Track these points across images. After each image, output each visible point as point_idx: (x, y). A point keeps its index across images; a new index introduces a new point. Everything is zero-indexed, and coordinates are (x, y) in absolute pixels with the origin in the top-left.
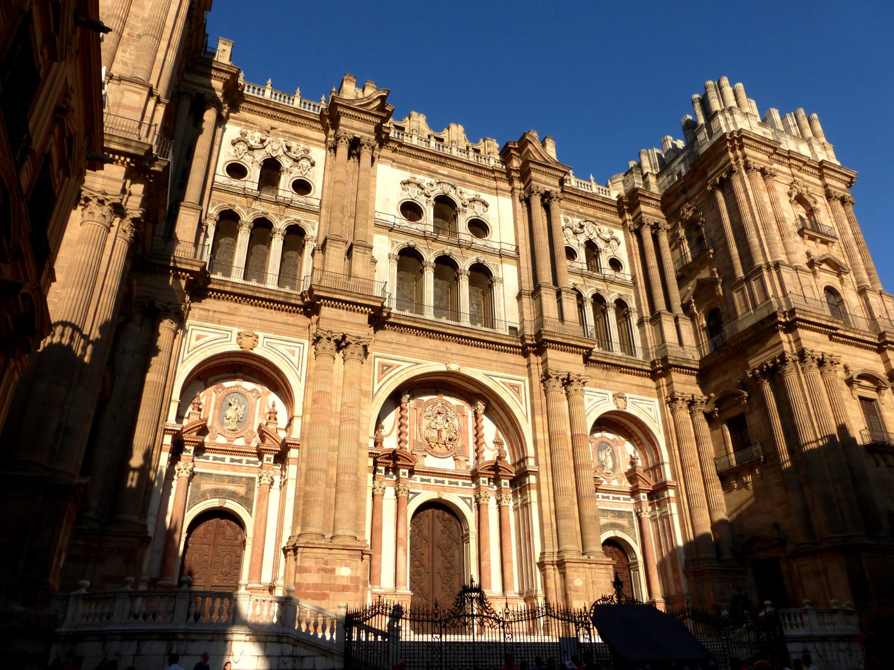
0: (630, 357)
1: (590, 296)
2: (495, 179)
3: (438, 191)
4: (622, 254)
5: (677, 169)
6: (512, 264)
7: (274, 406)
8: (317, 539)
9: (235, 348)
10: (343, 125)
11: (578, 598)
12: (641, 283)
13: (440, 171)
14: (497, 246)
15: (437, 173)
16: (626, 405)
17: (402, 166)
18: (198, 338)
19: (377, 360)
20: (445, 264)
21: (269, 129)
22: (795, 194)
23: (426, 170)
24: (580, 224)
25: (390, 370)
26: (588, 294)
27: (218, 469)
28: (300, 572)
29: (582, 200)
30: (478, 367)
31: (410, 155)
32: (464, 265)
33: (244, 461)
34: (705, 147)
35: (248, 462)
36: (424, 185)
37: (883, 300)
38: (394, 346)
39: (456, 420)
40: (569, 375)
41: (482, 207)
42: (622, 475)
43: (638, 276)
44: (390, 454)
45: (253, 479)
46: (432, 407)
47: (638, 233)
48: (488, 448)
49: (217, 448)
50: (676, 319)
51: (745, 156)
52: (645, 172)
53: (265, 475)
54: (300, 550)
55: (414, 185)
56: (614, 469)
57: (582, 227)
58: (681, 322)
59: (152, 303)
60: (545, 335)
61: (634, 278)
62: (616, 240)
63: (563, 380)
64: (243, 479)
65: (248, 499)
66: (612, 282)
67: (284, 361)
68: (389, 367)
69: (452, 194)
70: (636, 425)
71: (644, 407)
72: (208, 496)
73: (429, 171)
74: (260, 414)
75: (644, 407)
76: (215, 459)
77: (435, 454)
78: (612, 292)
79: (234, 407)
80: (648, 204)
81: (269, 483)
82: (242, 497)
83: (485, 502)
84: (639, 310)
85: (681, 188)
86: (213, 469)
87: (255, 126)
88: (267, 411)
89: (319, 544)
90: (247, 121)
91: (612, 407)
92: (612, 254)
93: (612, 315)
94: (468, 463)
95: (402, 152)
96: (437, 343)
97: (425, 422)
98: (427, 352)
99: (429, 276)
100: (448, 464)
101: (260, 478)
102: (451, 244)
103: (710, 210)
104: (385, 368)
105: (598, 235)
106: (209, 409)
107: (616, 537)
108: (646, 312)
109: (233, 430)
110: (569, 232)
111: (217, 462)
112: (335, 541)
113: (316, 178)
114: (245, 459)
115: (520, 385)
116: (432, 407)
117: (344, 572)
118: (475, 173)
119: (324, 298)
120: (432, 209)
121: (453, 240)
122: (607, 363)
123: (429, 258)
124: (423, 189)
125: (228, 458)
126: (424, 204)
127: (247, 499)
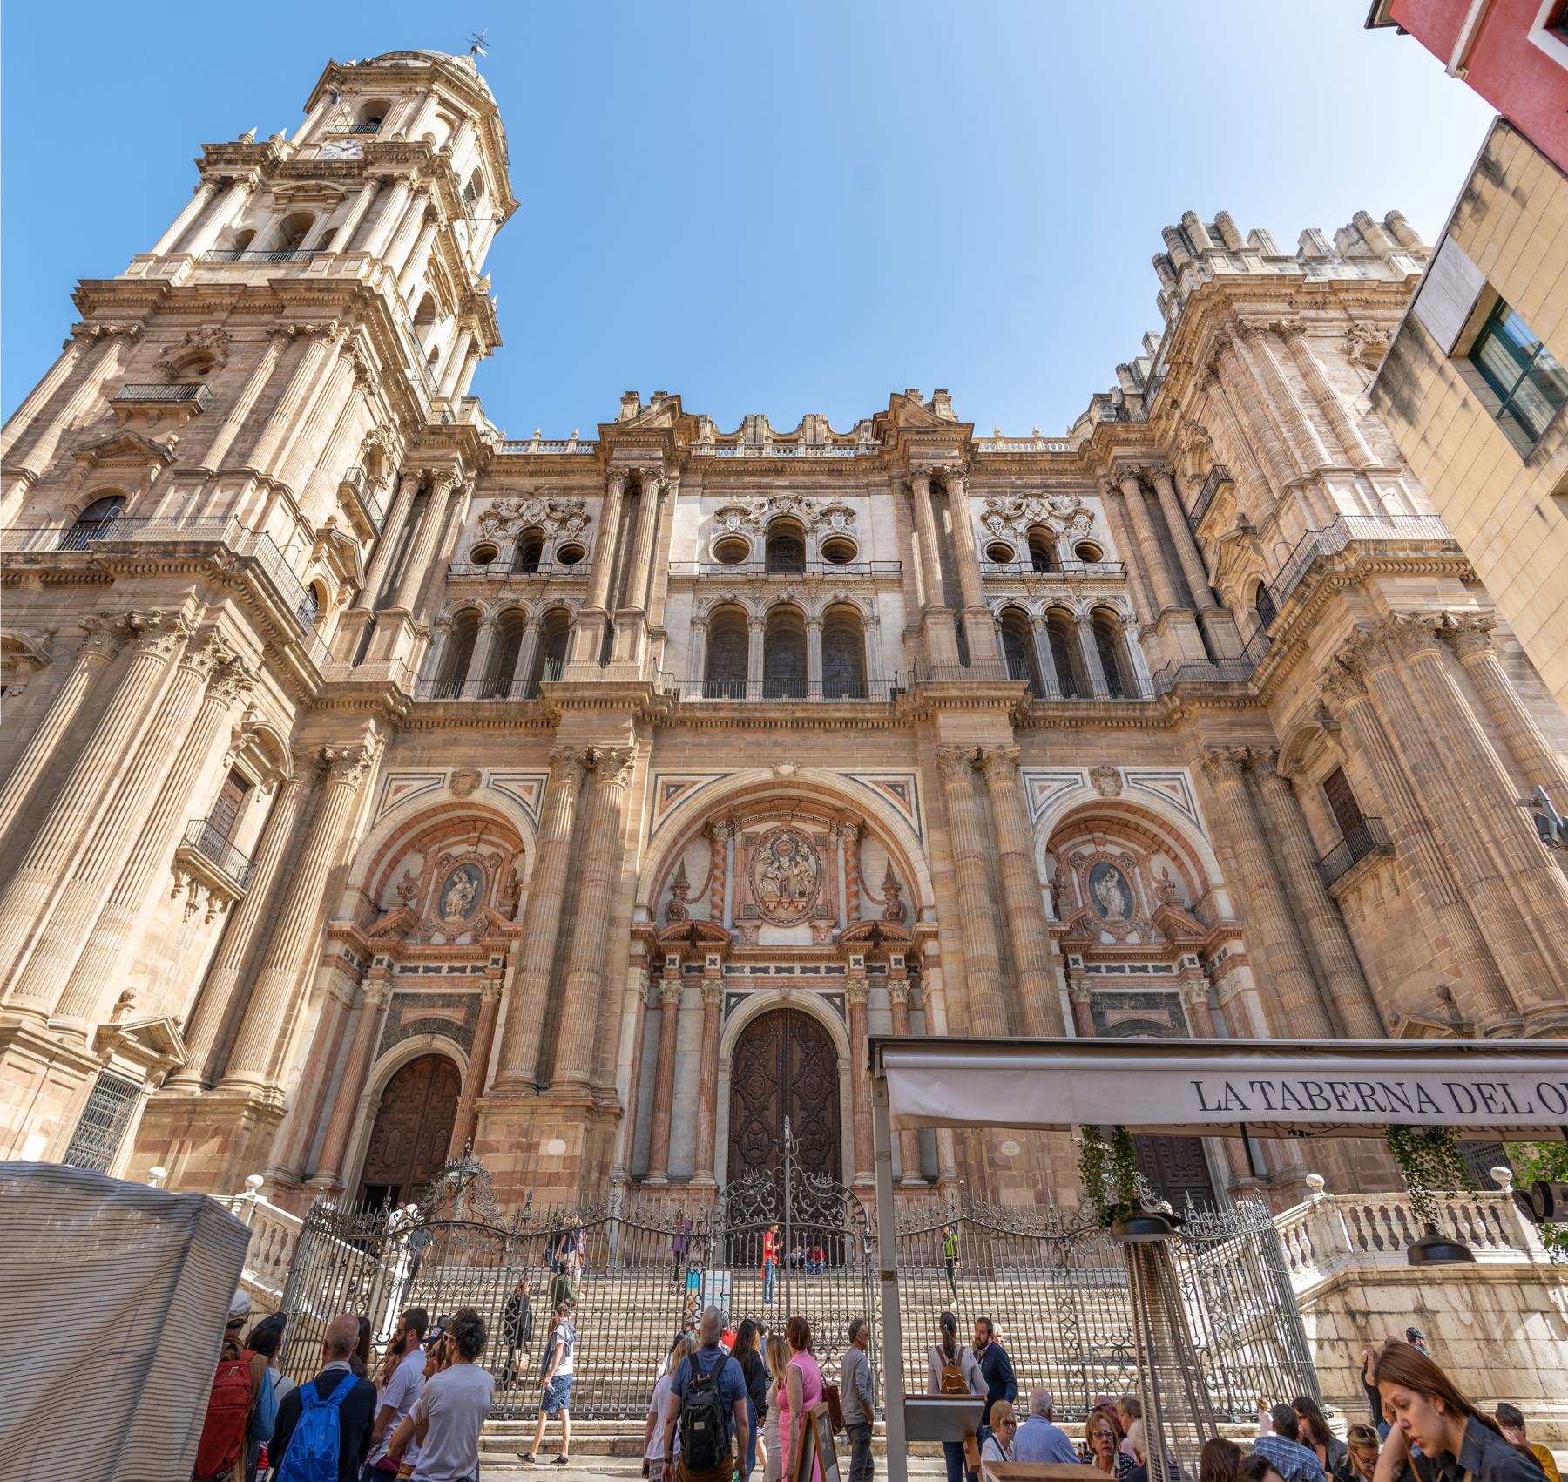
3: (775, 510)
7: (515, 872)
11: (1012, 1183)
14: (866, 569)
17: (718, 490)
31: (729, 472)
32: (814, 610)
36: (751, 508)
39: (812, 859)
41: (843, 518)
48: (873, 900)
69: (796, 511)
83: (860, 999)
94: (836, 932)
95: (717, 472)
96: (760, 736)
97: (760, 868)
98: (742, 754)
100: (799, 936)
102: (791, 584)
113: (587, 540)
117: (554, 1147)
118: (832, 472)
120: (763, 540)
121: (796, 577)
123: (756, 610)
126: (751, 536)
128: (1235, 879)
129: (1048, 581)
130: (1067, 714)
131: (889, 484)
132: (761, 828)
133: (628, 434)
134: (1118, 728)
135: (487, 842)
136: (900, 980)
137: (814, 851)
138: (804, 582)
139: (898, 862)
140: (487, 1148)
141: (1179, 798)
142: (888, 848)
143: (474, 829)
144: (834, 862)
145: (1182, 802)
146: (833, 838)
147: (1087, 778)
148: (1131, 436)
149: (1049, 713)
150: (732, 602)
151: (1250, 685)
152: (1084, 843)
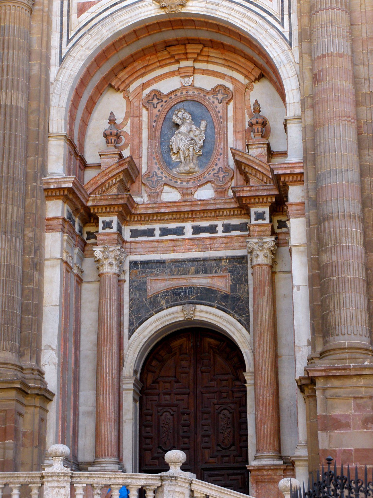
7: (257, 109)
8: (353, 359)
18: (82, 9)
27: (174, 251)
28: (325, 429)
33: (220, 229)
35: (227, 228)
45: (242, 259)
49: (162, 210)
53: (256, 247)
54: (320, 384)
64: (223, 263)
65: (239, 299)
67: (249, 14)
72: (163, 302)
76: (165, 232)
79: (183, 129)
81: (268, 261)
82: (225, 297)
86: (165, 251)
89: (355, 368)
101: (251, 253)
106: (141, 142)
109: (189, 173)
111: (170, 237)
114: (220, 224)
125: (188, 226)
127: (236, 299)
135: (205, 72)
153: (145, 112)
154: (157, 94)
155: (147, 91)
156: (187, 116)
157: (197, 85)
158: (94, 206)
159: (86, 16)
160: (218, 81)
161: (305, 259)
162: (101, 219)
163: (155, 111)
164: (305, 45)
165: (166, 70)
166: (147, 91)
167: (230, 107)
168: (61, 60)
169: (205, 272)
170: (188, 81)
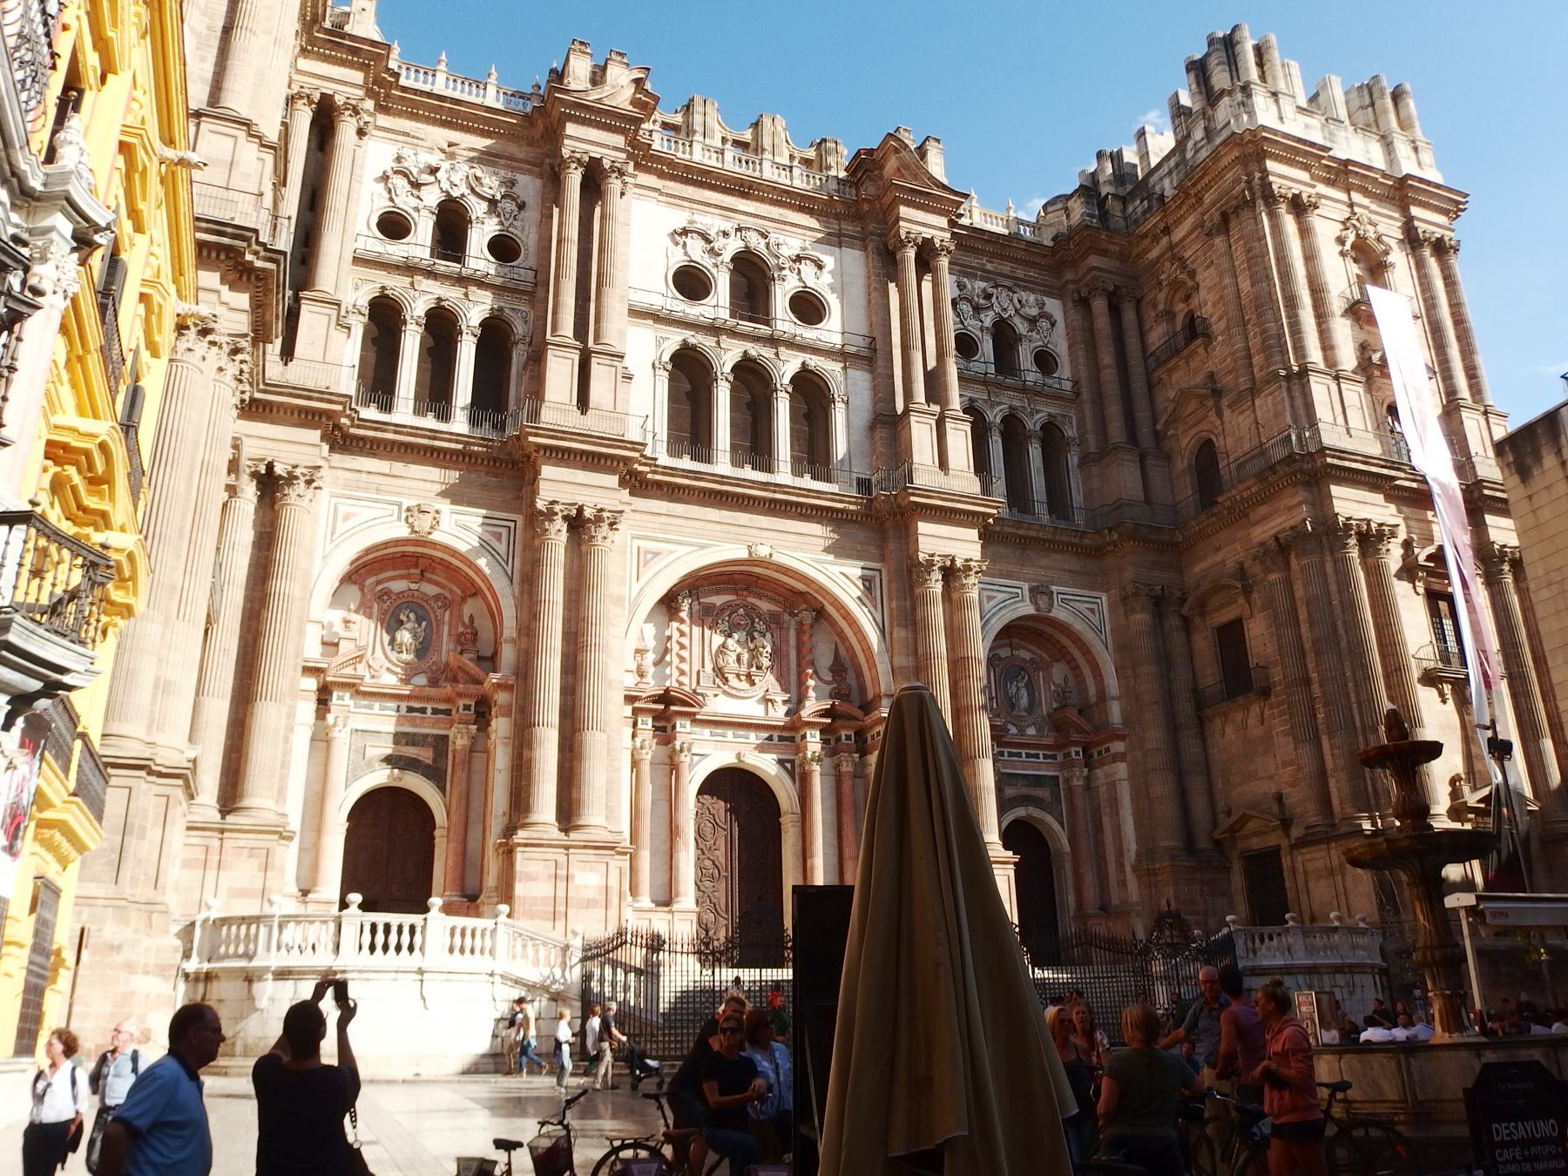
0: (1062, 525)
1: (998, 420)
2: (838, 217)
4: (1060, 345)
5: (1157, 188)
6: (863, 369)
9: (403, 532)
10: (571, 137)
12: (1086, 396)
13: (741, 208)
15: (735, 211)
16: (1052, 605)
18: (346, 518)
19: (637, 543)
20: (750, 376)
21: (445, 146)
22: (1351, 238)
23: (716, 206)
24: (984, 290)
25: (658, 558)
26: (994, 416)
29: (990, 248)
30: (802, 550)
33: (429, 711)
34: (1204, 154)
35: (435, 711)
36: (712, 233)
37: (1488, 422)
38: (663, 519)
40: (953, 561)
42: (1043, 717)
43: (1084, 382)
44: (660, 695)
46: (730, 616)
47: (1084, 304)
50: (1142, 458)
51: (1265, 173)
52: (1103, 195)
55: (695, 235)
56: (1030, 709)
57: (988, 297)
58: (1150, 462)
59: (270, 466)
60: (913, 495)
61: (1076, 383)
62: (1048, 317)
63: (942, 569)
66: (1038, 394)
68: (656, 554)
70: (1068, 637)
71: (1082, 607)
73: (722, 208)
74: (450, 635)
75: (1082, 607)
77: (734, 692)
78: (1038, 412)
80: (1104, 253)
82: (428, 766)
84: (1082, 442)
85: (1162, 225)
87: (420, 142)
88: (461, 629)
90: (408, 135)
91: (1027, 609)
92: (1040, 343)
93: (1035, 453)
98: (718, 527)
99: (723, 396)
103: (1208, 267)
104: (649, 556)
105: (1016, 310)
107: (1029, 816)
108: (1092, 446)
110: (965, 307)
112: (573, 835)
115: (874, 577)
116: (730, 616)
119: (546, 448)
121: (764, 330)
122: (1021, 537)
124: (708, 241)
126: (714, 271)
128: (1130, 694)
129: (1008, 388)
130: (1021, 532)
131: (863, 240)
132: (718, 600)
133: (587, 108)
134: (1054, 551)
135: (430, 581)
136: (850, 753)
137: (769, 629)
138: (773, 341)
139: (850, 649)
140: (530, 878)
141: (1095, 619)
142: (841, 634)
143: (416, 566)
144: (787, 641)
145: (1097, 624)
146: (786, 617)
147: (1026, 593)
148: (1112, 247)
149: (1006, 529)
150: (694, 348)
151: (1177, 532)
152: (1002, 646)
153: (376, 606)
154: (387, 592)
155: (379, 588)
156: (412, 616)
157: (422, 589)
158: (332, 683)
159: (349, 524)
160: (441, 591)
161: (509, 750)
162: (335, 695)
163: (385, 606)
164: (526, 587)
165: (397, 573)
166: (379, 588)
167: (447, 614)
168: (324, 557)
169: (414, 744)
170: (413, 586)
